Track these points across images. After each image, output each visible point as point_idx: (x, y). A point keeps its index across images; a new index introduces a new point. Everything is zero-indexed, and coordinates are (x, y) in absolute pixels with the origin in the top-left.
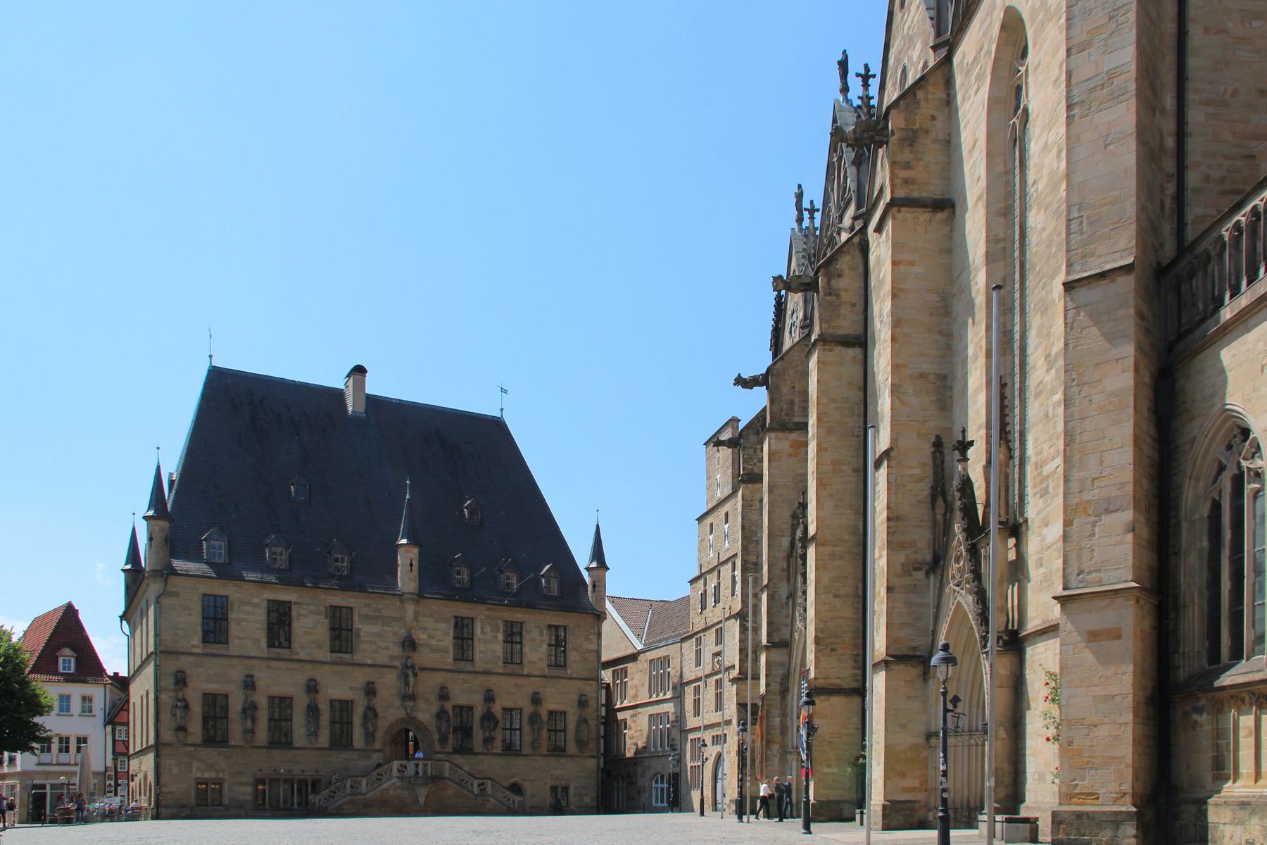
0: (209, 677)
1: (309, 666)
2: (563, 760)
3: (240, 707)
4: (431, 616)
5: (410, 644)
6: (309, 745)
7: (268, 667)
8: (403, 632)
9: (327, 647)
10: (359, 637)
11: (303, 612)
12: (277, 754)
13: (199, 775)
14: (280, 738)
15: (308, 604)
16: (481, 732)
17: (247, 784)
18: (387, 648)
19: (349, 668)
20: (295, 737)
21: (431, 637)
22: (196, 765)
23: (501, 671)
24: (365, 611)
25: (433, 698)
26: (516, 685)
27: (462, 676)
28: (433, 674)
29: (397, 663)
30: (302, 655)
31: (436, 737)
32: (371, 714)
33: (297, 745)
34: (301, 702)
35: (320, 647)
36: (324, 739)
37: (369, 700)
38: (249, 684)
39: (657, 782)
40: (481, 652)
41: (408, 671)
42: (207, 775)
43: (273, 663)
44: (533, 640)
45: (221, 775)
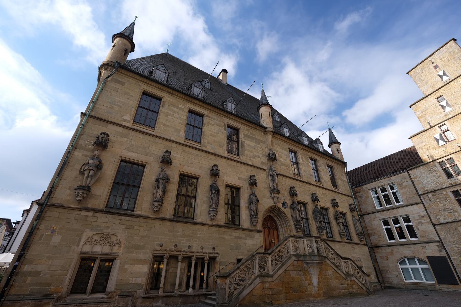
0: (127, 146)
1: (213, 157)
3: (154, 178)
6: (209, 222)
7: (184, 151)
8: (267, 151)
10: (243, 146)
11: (211, 122)
12: (179, 227)
13: (87, 248)
14: (184, 215)
15: (214, 119)
16: (314, 223)
18: (259, 157)
19: (239, 165)
20: (198, 211)
21: (281, 157)
22: (88, 233)
23: (314, 183)
24: (246, 132)
25: (287, 194)
26: (323, 194)
28: (284, 179)
29: (265, 168)
30: (208, 149)
31: (292, 223)
32: (253, 201)
33: (199, 220)
34: (205, 183)
35: (220, 146)
36: (222, 216)
37: (251, 189)
38: (166, 161)
39: (403, 262)
40: (304, 171)
41: (274, 176)
42: (98, 249)
43: (187, 149)
44: (323, 170)
45: (115, 250)
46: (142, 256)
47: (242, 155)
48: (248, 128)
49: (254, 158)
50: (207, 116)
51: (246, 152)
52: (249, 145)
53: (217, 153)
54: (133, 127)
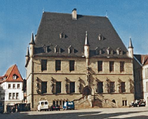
2: (125, 94)
4: (92, 61)
5: (89, 69)
9: (69, 70)
10: (76, 67)
17: (52, 102)
18: (83, 69)
27: (100, 75)
29: (85, 73)
35: (67, 70)
46: (51, 102)
47: (76, 70)
48: (78, 59)
49: (80, 70)
50: (62, 61)
51: (77, 69)
52: (79, 66)
53: (67, 73)
54: (43, 73)
